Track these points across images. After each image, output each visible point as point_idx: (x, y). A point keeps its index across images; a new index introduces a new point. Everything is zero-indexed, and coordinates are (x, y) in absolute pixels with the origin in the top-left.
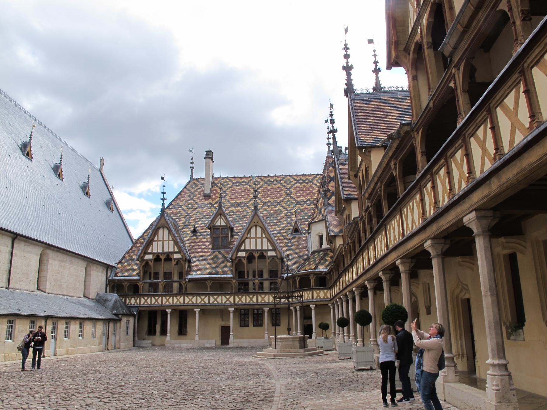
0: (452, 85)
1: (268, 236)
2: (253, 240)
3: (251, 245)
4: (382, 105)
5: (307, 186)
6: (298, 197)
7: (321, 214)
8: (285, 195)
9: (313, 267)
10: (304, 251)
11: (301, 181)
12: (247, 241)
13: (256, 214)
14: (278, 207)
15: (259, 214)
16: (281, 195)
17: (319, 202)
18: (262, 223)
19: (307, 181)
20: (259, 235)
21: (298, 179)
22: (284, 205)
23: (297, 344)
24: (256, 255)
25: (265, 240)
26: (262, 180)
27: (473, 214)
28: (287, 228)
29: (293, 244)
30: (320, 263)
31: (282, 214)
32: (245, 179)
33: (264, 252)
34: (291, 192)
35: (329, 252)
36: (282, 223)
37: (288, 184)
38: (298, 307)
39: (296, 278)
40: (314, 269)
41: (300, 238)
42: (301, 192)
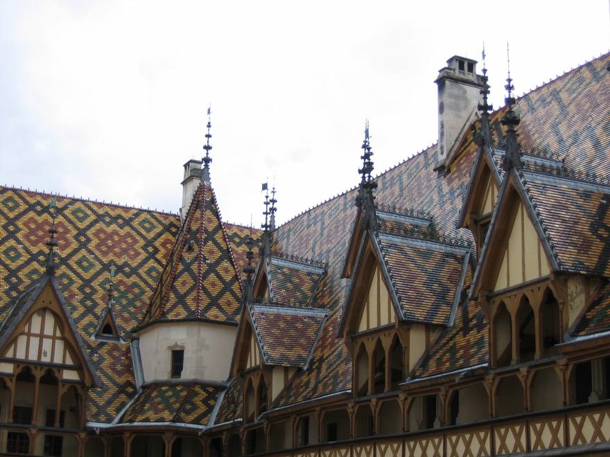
1: (68, 336)
2: (35, 342)
5: (122, 232)
6: (105, 254)
7: (186, 307)
11: (107, 219)
12: (22, 340)
13: (50, 284)
15: (58, 286)
17: (180, 280)
19: (120, 221)
20: (49, 330)
21: (101, 211)
22: (75, 267)
24: (38, 374)
25: (60, 345)
28: (86, 321)
29: (101, 359)
31: (74, 288)
33: (55, 370)
34: (89, 240)
35: (197, 389)
36: (74, 308)
39: (127, 435)
40: (173, 421)
41: (115, 348)
42: (110, 243)
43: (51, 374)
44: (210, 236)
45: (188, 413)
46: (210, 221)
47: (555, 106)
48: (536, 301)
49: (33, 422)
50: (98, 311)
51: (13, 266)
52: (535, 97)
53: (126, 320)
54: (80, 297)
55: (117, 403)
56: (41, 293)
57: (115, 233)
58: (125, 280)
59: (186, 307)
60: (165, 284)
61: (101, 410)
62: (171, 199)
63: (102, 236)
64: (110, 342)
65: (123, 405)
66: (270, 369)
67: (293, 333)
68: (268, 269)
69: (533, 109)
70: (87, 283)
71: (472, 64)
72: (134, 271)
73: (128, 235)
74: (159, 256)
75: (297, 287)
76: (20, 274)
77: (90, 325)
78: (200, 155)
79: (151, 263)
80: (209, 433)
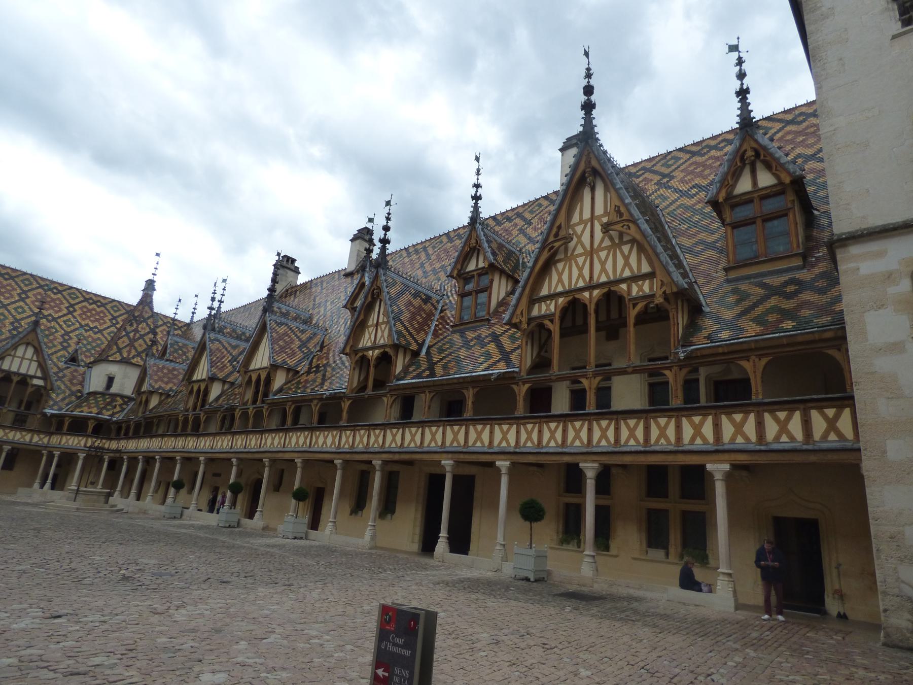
0: (385, 399)
1: (41, 360)
2: (17, 361)
3: (11, 365)
4: (289, 332)
5: (98, 310)
6: (83, 319)
7: (121, 354)
8: (65, 311)
9: (95, 410)
10: (76, 388)
14: (53, 323)
15: (39, 331)
16: (60, 310)
18: (39, 343)
21: (87, 297)
22: (62, 323)
23: (102, 499)
24: (16, 379)
25: (34, 365)
26: (36, 281)
27: (380, 462)
28: (60, 354)
29: (64, 376)
30: (104, 408)
31: (58, 335)
32: (9, 271)
34: (75, 311)
35: (118, 399)
36: (54, 346)
37: (73, 299)
38: (57, 453)
41: (76, 371)
42: (89, 314)
43: (24, 380)
44: (145, 320)
45: (108, 410)
46: (147, 312)
47: (319, 288)
48: (263, 378)
49: (6, 406)
50: (70, 350)
51: (18, 317)
52: (314, 282)
53: (88, 357)
54: (61, 340)
55: (67, 401)
56: (27, 334)
57: (94, 309)
58: (93, 335)
59: (121, 354)
60: (114, 341)
61: (56, 403)
62: (132, 298)
63: (85, 310)
64: (73, 368)
65: (71, 403)
66: (151, 393)
67: (171, 376)
68: (169, 342)
69: (311, 288)
70: (67, 333)
71: (293, 261)
72: (100, 331)
73: (102, 312)
74: (118, 326)
75: (184, 354)
76: (22, 322)
77: (63, 356)
78: (151, 277)
79: (113, 329)
80: (116, 422)
